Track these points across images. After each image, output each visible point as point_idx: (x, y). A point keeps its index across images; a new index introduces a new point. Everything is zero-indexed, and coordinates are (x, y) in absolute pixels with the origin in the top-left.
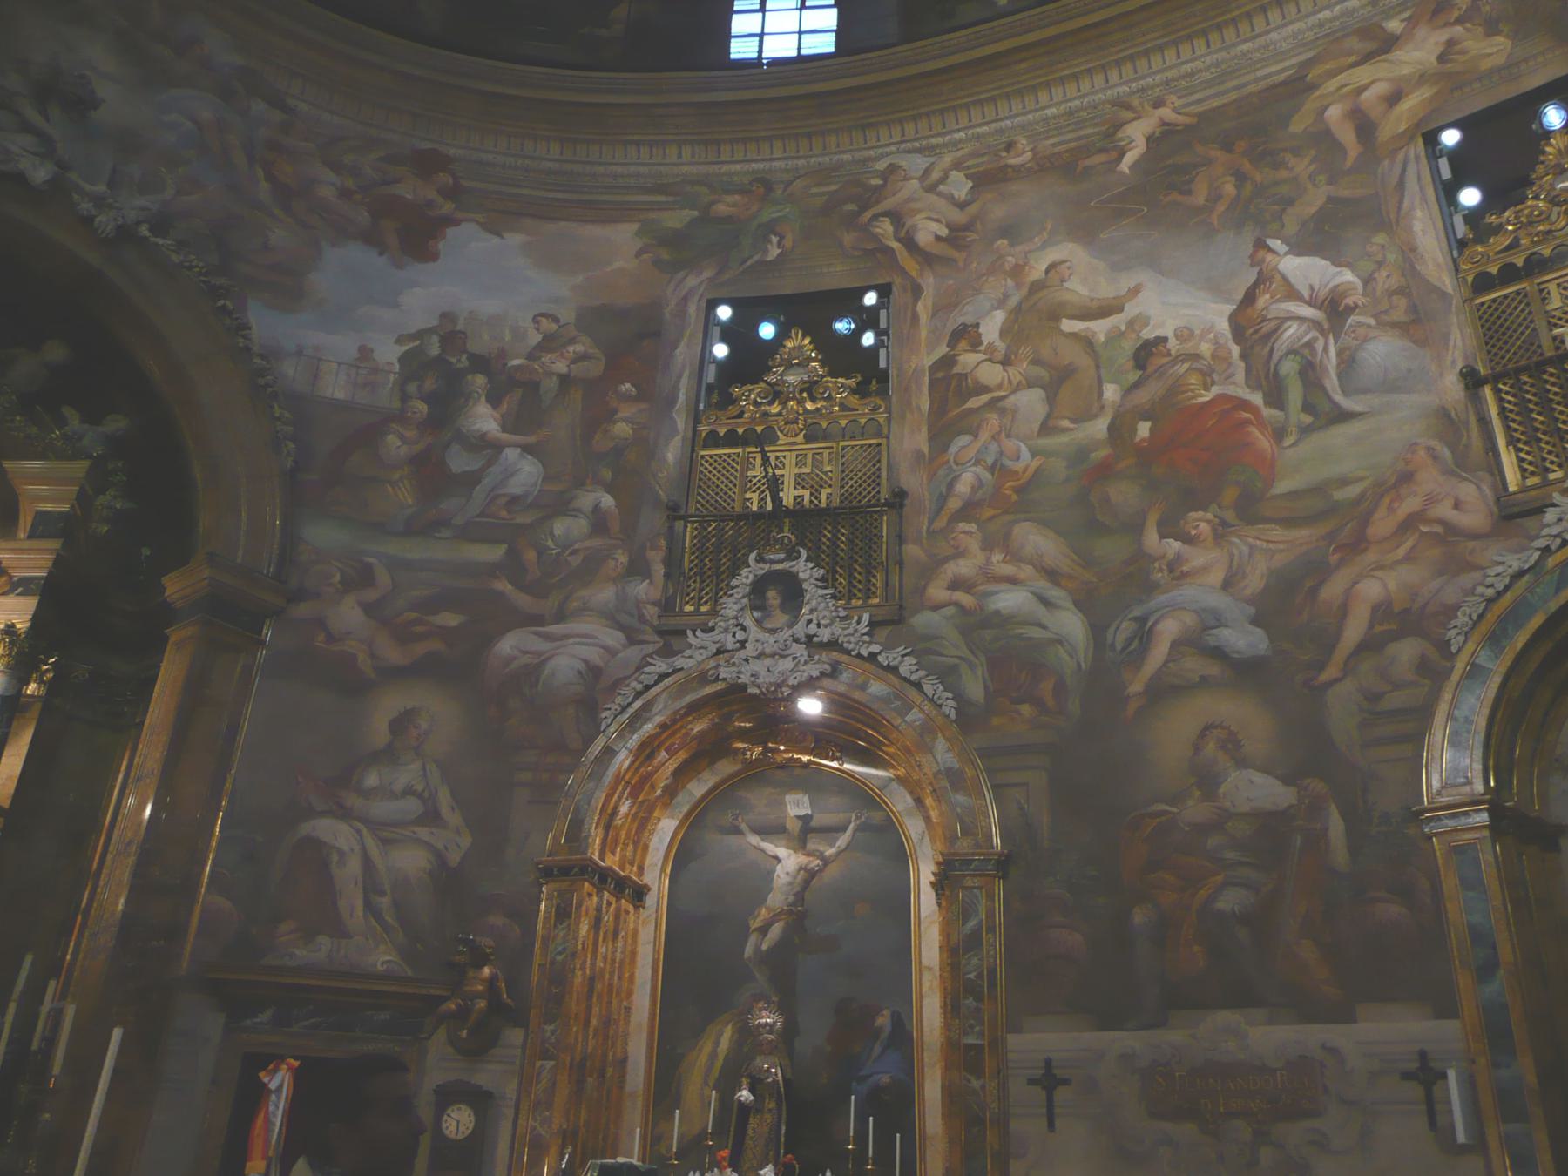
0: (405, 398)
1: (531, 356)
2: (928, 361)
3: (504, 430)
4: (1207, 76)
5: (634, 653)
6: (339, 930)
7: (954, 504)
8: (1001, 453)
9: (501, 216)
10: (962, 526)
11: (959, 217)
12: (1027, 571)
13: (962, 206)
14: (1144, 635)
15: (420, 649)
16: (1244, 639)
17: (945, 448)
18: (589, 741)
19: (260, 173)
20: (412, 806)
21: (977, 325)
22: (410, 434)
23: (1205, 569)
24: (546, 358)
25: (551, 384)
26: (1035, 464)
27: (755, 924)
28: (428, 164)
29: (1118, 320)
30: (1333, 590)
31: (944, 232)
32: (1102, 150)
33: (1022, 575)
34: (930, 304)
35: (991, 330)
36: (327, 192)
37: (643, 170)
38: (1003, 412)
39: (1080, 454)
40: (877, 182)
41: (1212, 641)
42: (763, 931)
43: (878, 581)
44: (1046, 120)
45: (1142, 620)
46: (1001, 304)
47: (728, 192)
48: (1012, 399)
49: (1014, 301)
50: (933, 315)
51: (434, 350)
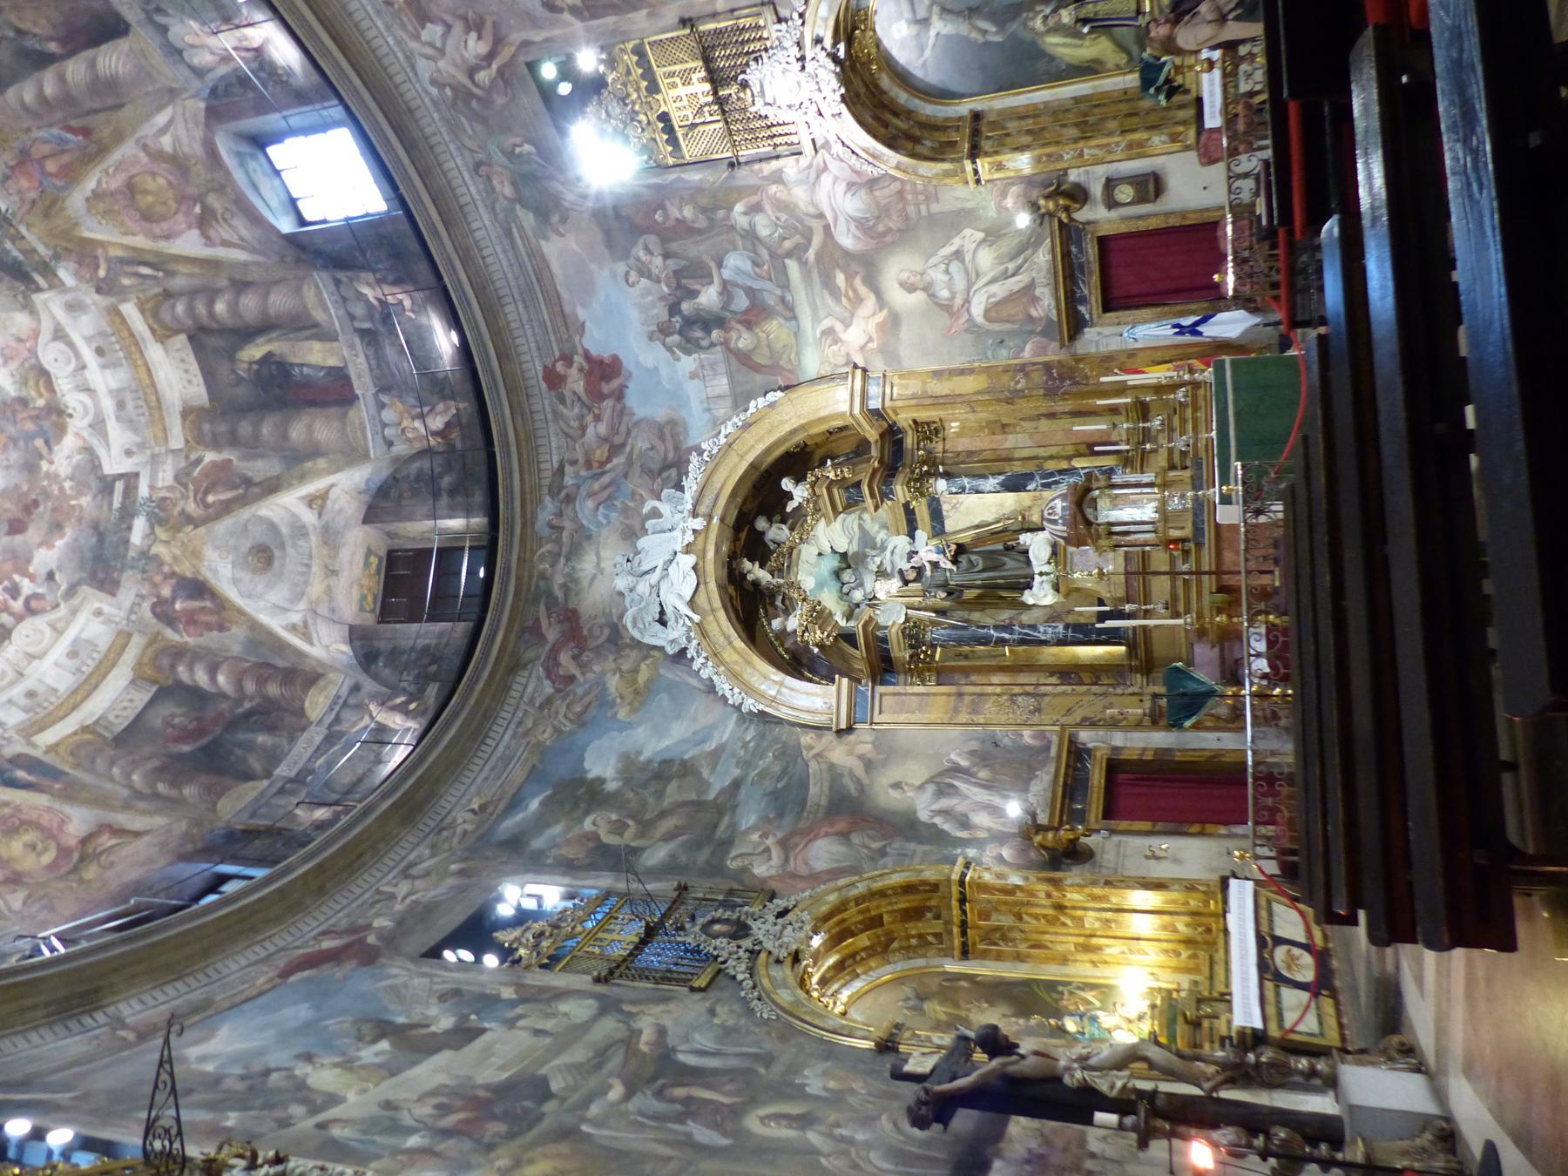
0: (712, 345)
1: (658, 281)
3: (711, 282)
5: (833, 166)
6: (1031, 286)
9: (568, 325)
11: (458, 27)
13: (449, 27)
15: (863, 290)
18: (895, 179)
19: (609, 466)
20: (955, 267)
22: (734, 335)
24: (655, 271)
25: (671, 263)
27: (981, 39)
28: (554, 380)
31: (473, 35)
36: (602, 429)
37: (499, 249)
40: (448, 91)
42: (984, 32)
43: (747, 22)
47: (493, 189)
50: (541, 28)
51: (676, 338)
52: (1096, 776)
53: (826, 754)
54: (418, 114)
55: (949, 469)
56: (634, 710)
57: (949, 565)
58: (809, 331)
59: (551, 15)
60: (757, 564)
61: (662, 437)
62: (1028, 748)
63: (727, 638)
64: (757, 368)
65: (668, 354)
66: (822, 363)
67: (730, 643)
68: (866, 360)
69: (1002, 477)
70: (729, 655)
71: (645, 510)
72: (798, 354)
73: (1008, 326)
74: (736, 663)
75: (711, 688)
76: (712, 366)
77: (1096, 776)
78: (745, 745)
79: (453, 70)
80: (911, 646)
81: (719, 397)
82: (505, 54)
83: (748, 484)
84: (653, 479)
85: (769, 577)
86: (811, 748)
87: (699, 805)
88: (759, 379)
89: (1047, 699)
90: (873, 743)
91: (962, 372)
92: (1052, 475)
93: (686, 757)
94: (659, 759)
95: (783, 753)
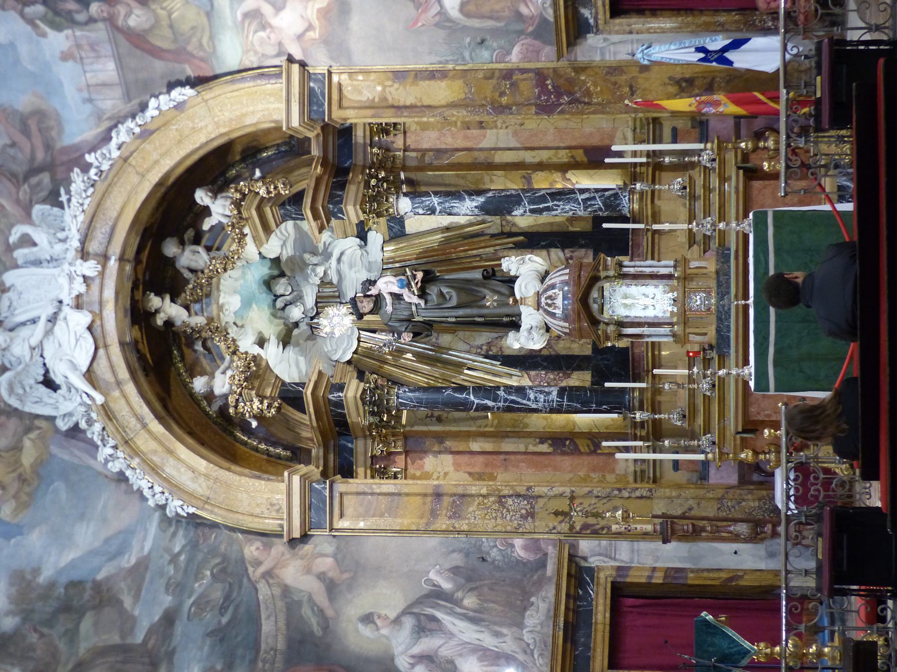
0: (92, 20)
22: (121, 10)
52: (601, 608)
53: (277, 571)
55: (413, 175)
56: (21, 506)
57: (415, 300)
58: (227, 11)
60: (168, 298)
61: (25, 131)
62: (519, 562)
63: (140, 419)
64: (156, 53)
65: (29, 28)
66: (246, 52)
67: (145, 426)
68: (304, 51)
69: (481, 199)
70: (143, 442)
71: (13, 239)
72: (212, 38)
73: (490, 23)
74: (155, 452)
75: (121, 478)
76: (93, 46)
77: (601, 608)
78: (174, 559)
80: (373, 413)
81: (104, 85)
83: (153, 203)
84: (18, 186)
85: (183, 313)
86: (258, 563)
87: (124, 650)
88: (159, 67)
89: (541, 502)
90: (335, 556)
91: (431, 75)
92: (543, 199)
93: (100, 577)
94: (64, 580)
95: (223, 571)
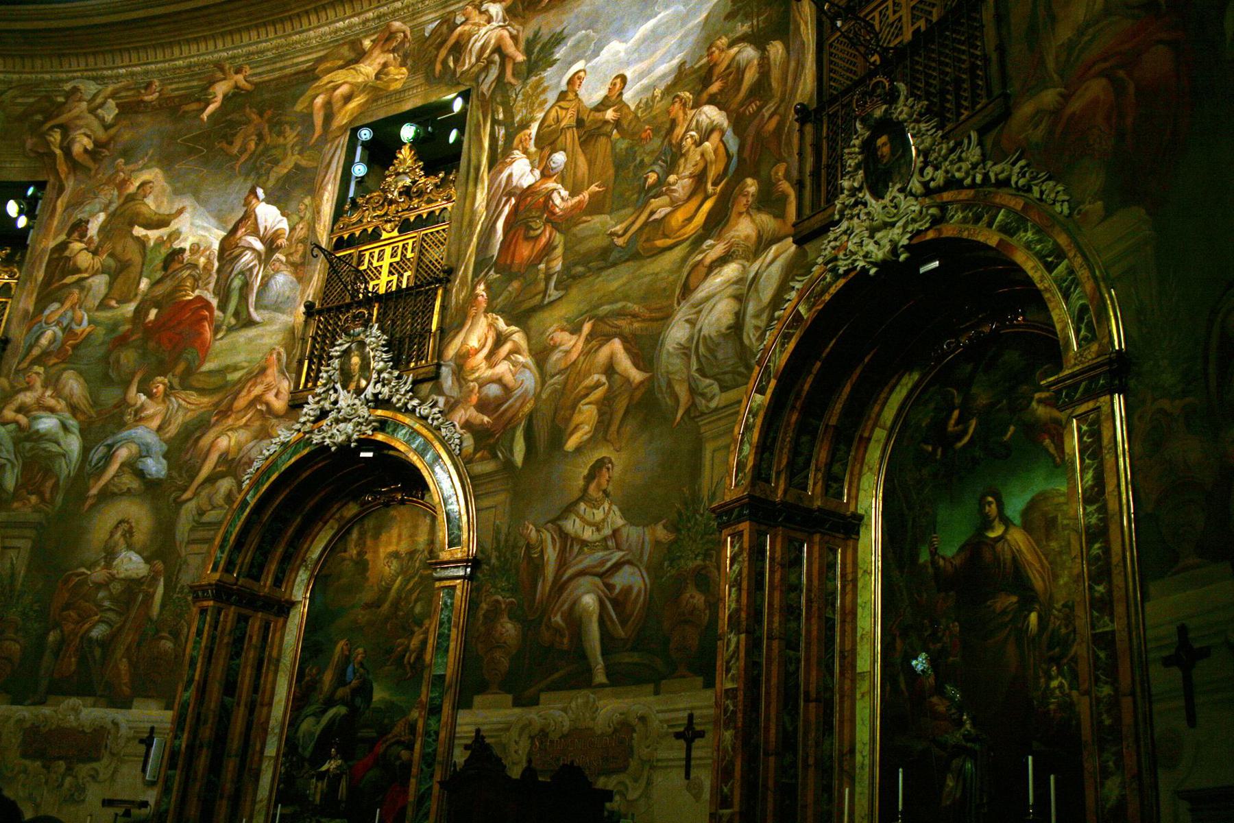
2: (52, 244)
4: (270, 55)
7: (36, 352)
8: (72, 319)
10: (36, 368)
11: (102, 135)
12: (61, 405)
14: (109, 457)
16: (155, 466)
17: (42, 311)
21: (87, 222)
23: (152, 417)
26: (88, 330)
29: (163, 232)
30: (205, 441)
31: (90, 146)
32: (198, 100)
33: (59, 408)
34: (66, 200)
35: (93, 228)
38: (82, 289)
39: (113, 326)
40: (61, 99)
41: (140, 466)
44: (175, 69)
45: (110, 446)
46: (104, 209)
48: (90, 280)
49: (112, 208)
54: (56, 62)
59: (70, 224)
79: (76, 112)
82: (62, 168)
